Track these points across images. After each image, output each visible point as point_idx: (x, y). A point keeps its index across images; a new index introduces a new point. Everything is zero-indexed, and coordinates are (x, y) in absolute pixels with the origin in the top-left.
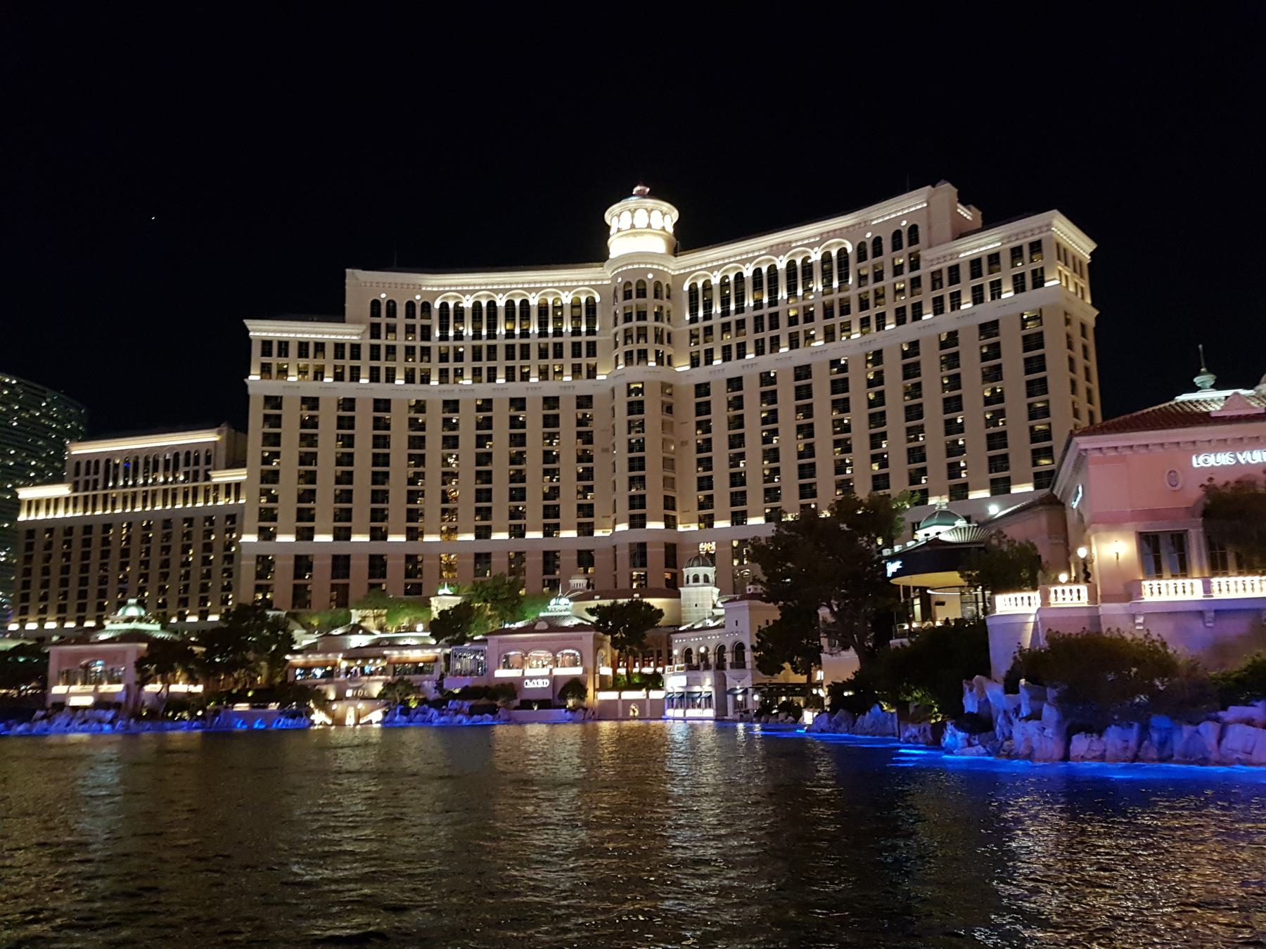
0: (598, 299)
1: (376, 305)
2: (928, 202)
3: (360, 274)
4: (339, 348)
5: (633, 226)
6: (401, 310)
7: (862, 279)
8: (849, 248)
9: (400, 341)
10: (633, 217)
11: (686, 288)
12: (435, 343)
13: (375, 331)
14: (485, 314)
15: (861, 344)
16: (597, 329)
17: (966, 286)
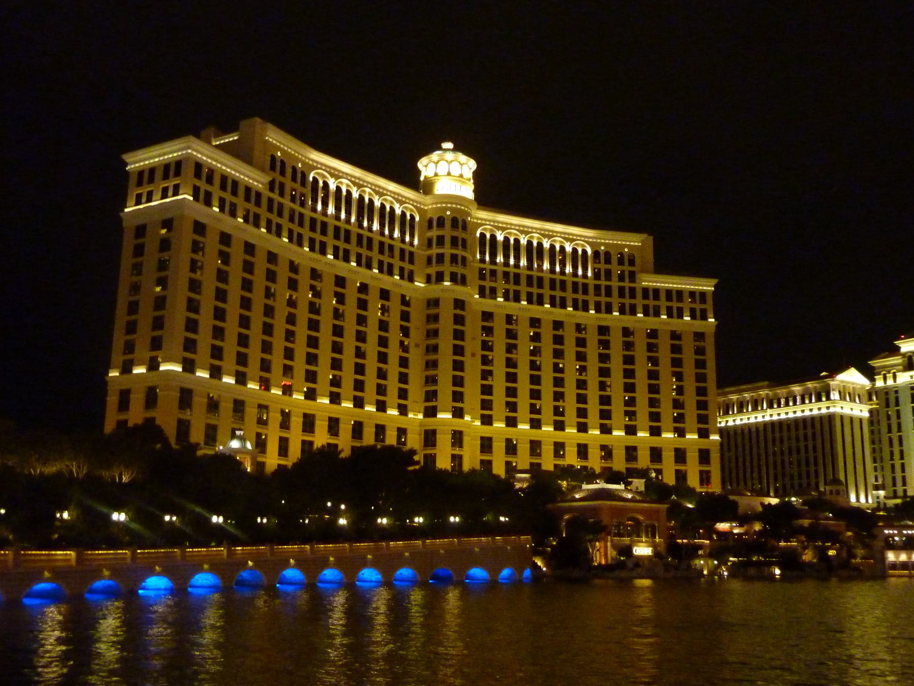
0: (417, 219)
2: (642, 242)
3: (269, 126)
4: (248, 189)
5: (461, 176)
6: (289, 171)
7: (597, 275)
8: (589, 251)
9: (287, 202)
10: (461, 168)
11: (478, 235)
12: (308, 213)
13: (271, 186)
14: (342, 199)
15: (597, 318)
16: (416, 242)
17: (663, 303)
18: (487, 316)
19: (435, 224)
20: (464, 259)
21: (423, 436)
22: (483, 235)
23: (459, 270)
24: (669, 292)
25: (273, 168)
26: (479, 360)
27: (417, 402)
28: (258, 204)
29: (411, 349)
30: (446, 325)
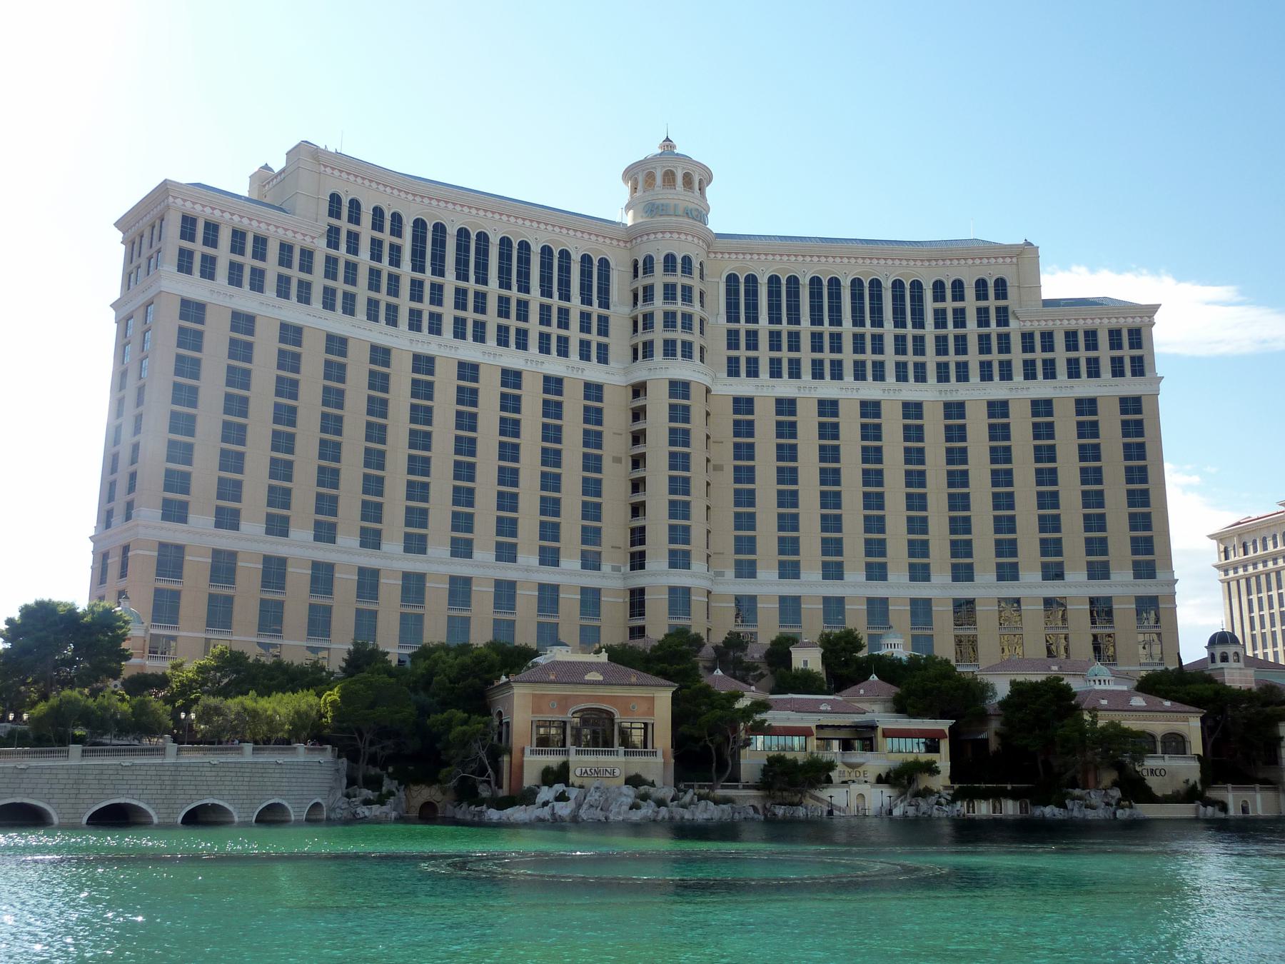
0: (612, 264)
1: (335, 199)
4: (286, 249)
13: (333, 237)
18: (744, 404)
19: (641, 264)
20: (687, 318)
21: (628, 599)
22: (732, 280)
23: (679, 335)
24: (1071, 337)
25: (334, 211)
26: (729, 474)
27: (620, 548)
28: (307, 266)
29: (607, 463)
30: (658, 423)
